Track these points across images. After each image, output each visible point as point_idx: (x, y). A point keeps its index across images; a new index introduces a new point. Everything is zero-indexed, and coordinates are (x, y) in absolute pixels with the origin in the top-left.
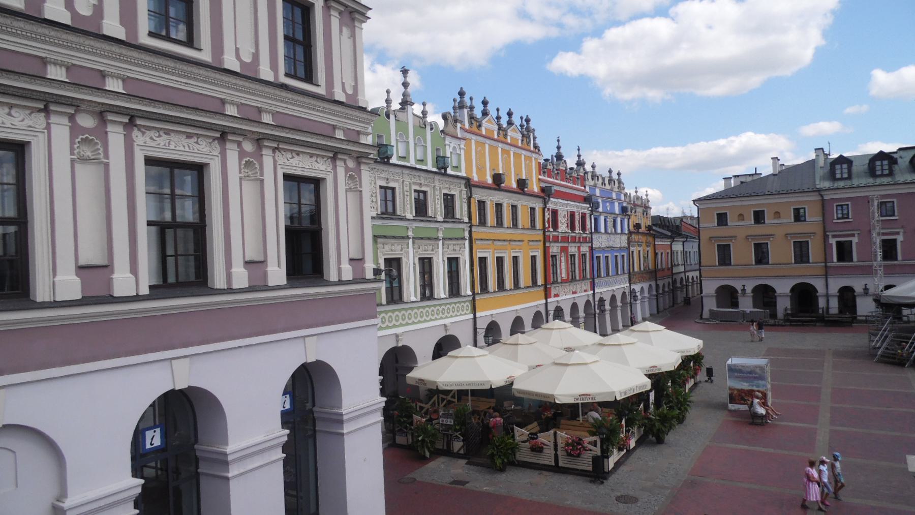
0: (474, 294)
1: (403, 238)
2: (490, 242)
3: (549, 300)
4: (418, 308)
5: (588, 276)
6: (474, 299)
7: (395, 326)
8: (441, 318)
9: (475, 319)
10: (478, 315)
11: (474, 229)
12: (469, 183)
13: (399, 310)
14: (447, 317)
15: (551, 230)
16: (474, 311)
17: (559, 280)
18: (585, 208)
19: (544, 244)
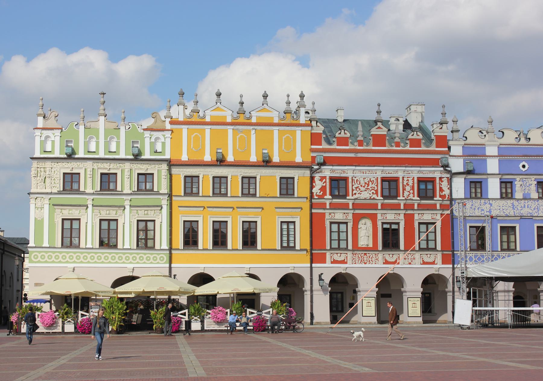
0: (171, 249)
1: (80, 206)
2: (202, 209)
3: (314, 265)
4: (96, 253)
5: (439, 247)
6: (171, 254)
7: (67, 262)
8: (124, 263)
9: (170, 268)
10: (173, 265)
11: (174, 198)
12: (171, 164)
13: (75, 253)
14: (131, 263)
15: (328, 196)
16: (170, 263)
17: (350, 247)
18: (434, 171)
19: (311, 210)
